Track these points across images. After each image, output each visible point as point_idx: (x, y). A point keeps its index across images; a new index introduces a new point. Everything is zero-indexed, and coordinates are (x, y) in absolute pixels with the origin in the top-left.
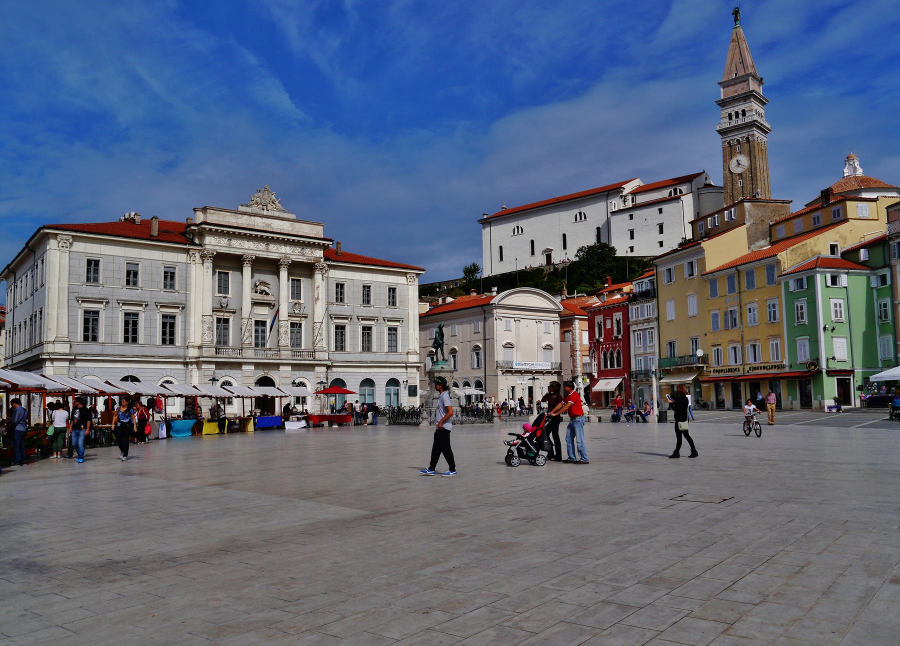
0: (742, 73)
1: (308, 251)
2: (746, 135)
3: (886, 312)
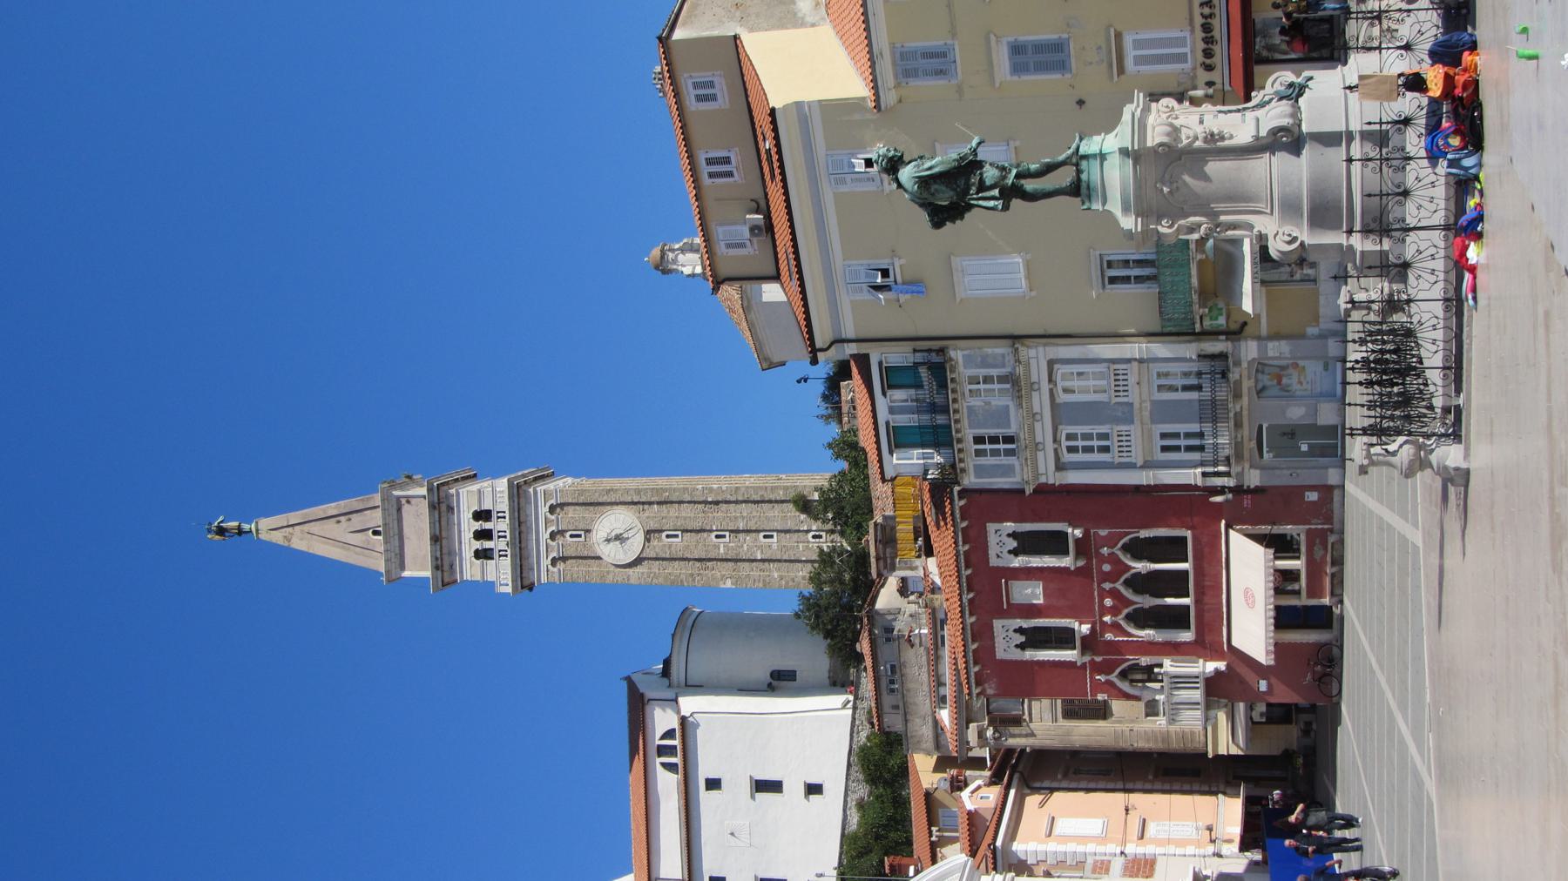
0: (378, 513)
2: (543, 509)
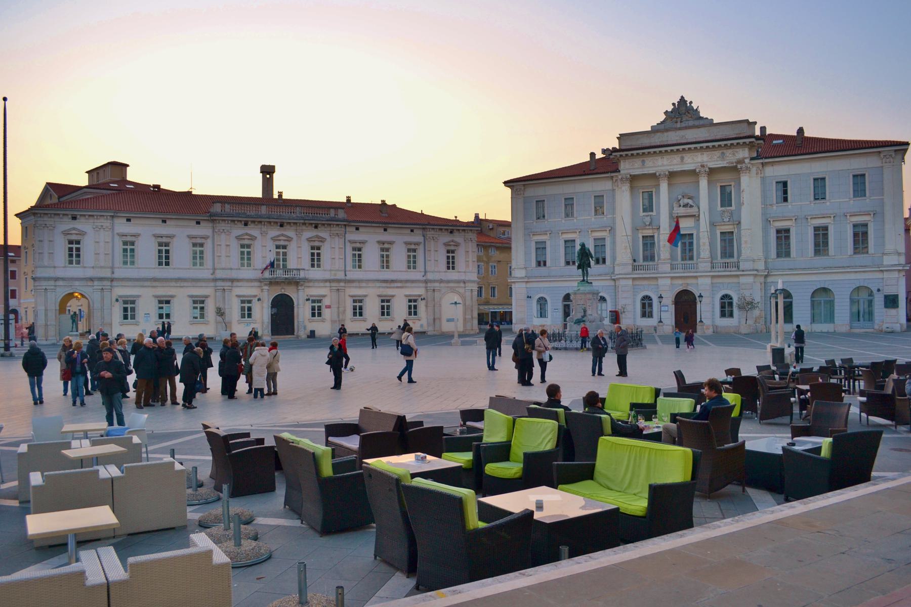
1: (728, 152)
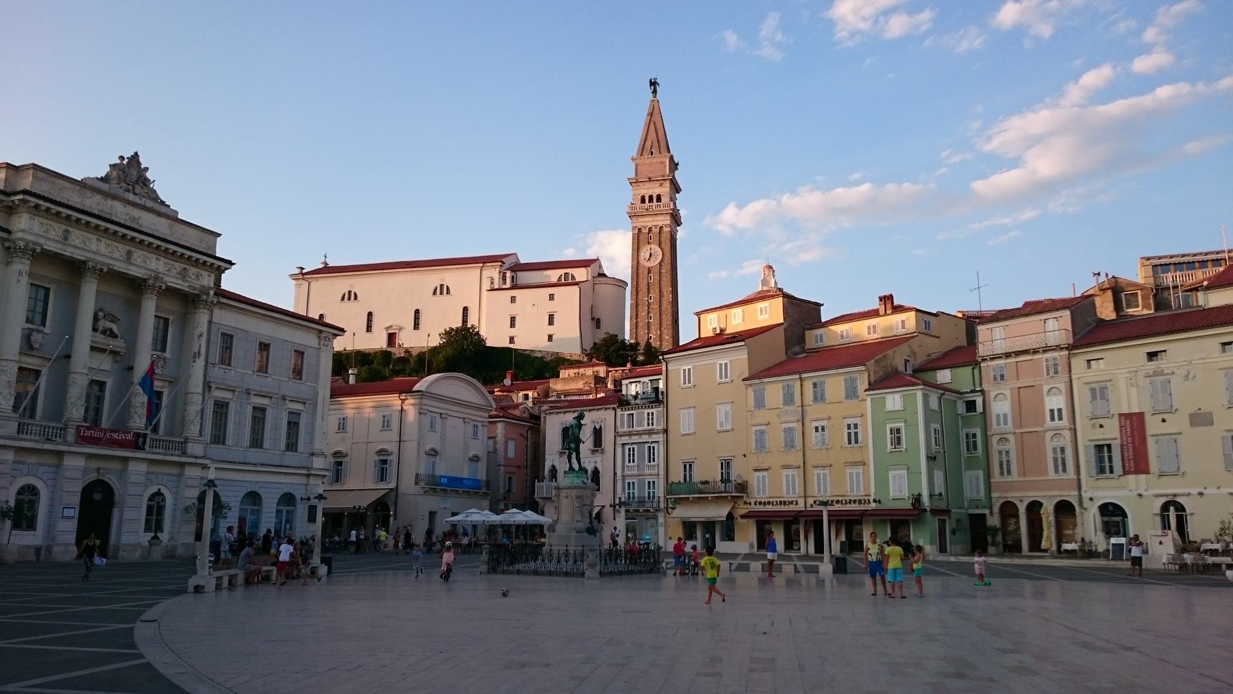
1: (193, 270)
2: (661, 224)
3: (975, 443)
